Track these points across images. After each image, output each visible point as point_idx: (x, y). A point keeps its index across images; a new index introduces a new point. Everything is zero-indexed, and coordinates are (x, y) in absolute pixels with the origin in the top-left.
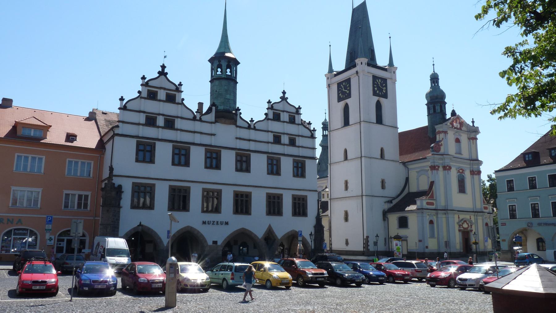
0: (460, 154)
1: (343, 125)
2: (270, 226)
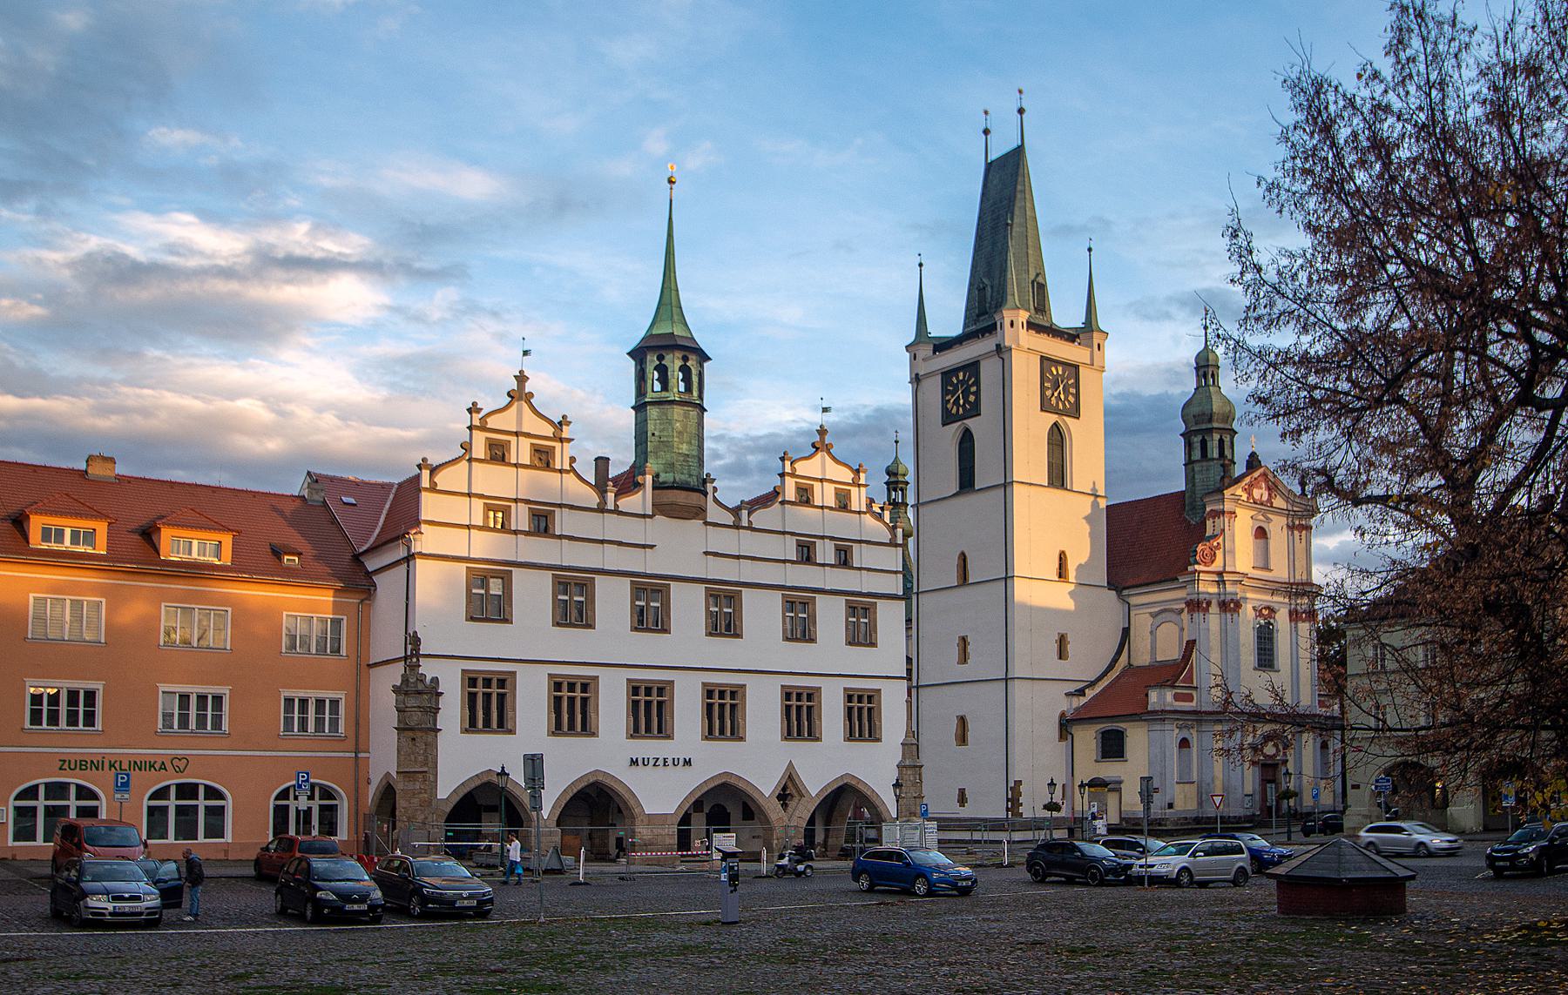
0: (1266, 568)
1: (955, 488)
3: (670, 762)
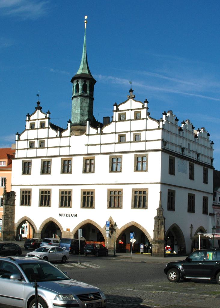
2: (111, 218)
3: (70, 215)
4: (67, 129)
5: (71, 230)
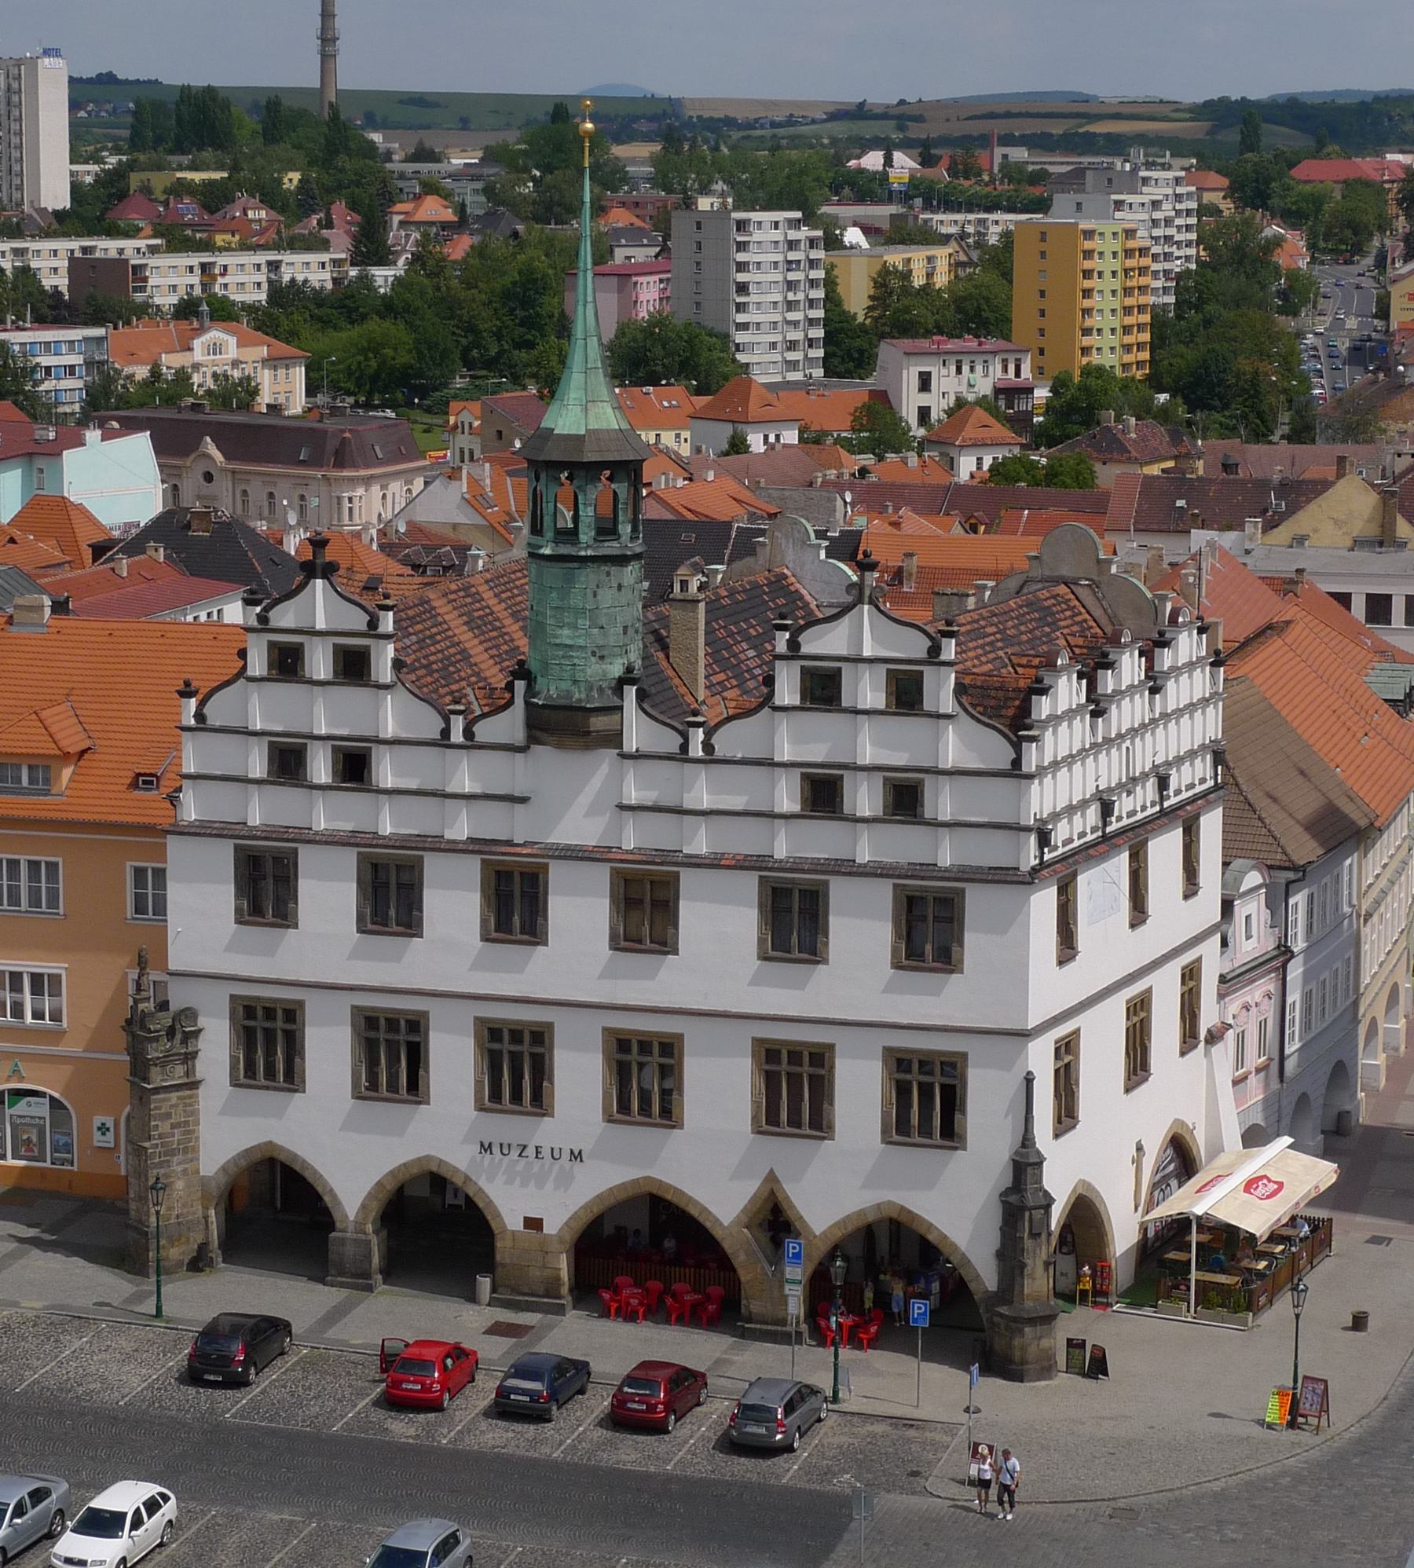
3: (546, 1153)
4: (510, 703)
5: (551, 1228)
